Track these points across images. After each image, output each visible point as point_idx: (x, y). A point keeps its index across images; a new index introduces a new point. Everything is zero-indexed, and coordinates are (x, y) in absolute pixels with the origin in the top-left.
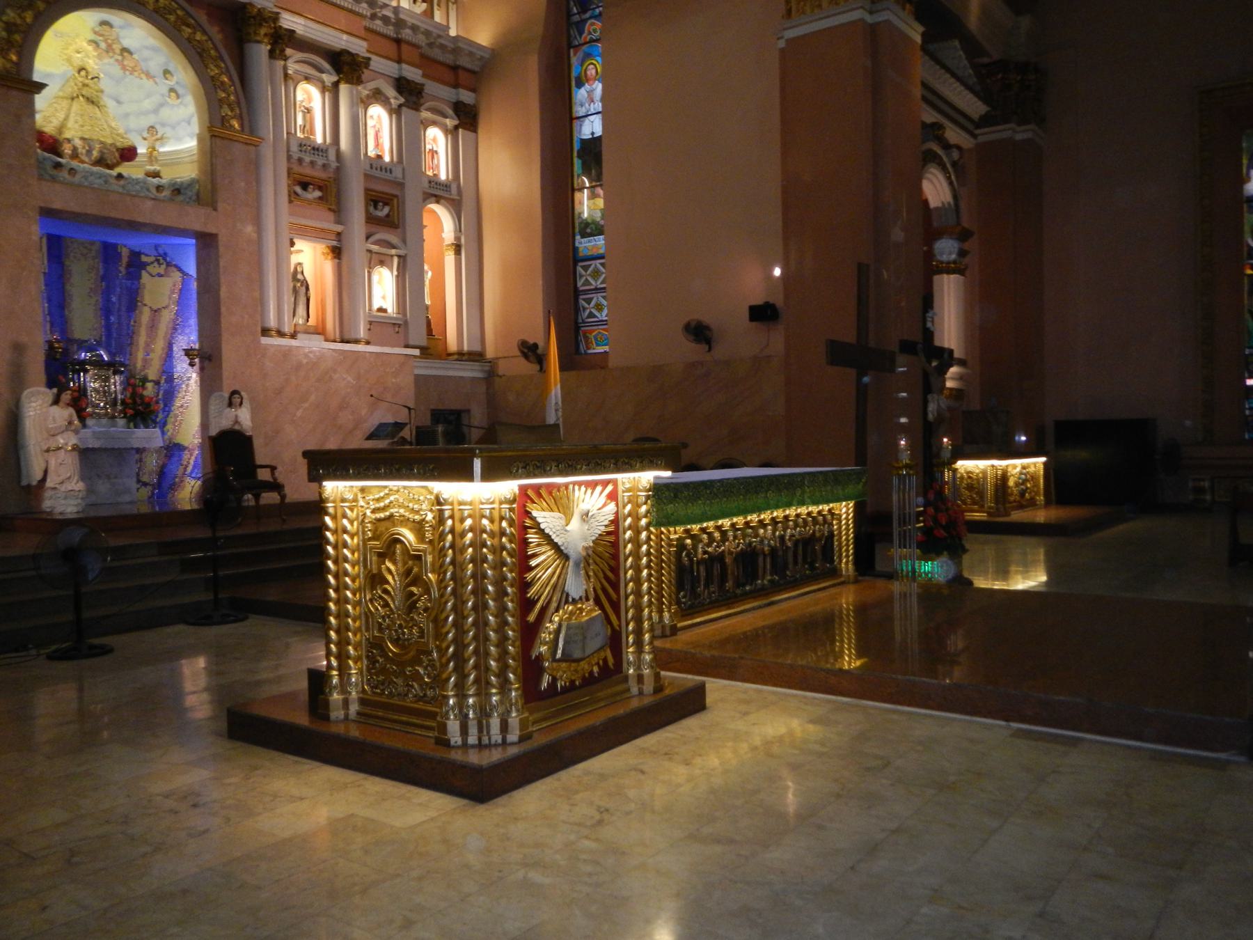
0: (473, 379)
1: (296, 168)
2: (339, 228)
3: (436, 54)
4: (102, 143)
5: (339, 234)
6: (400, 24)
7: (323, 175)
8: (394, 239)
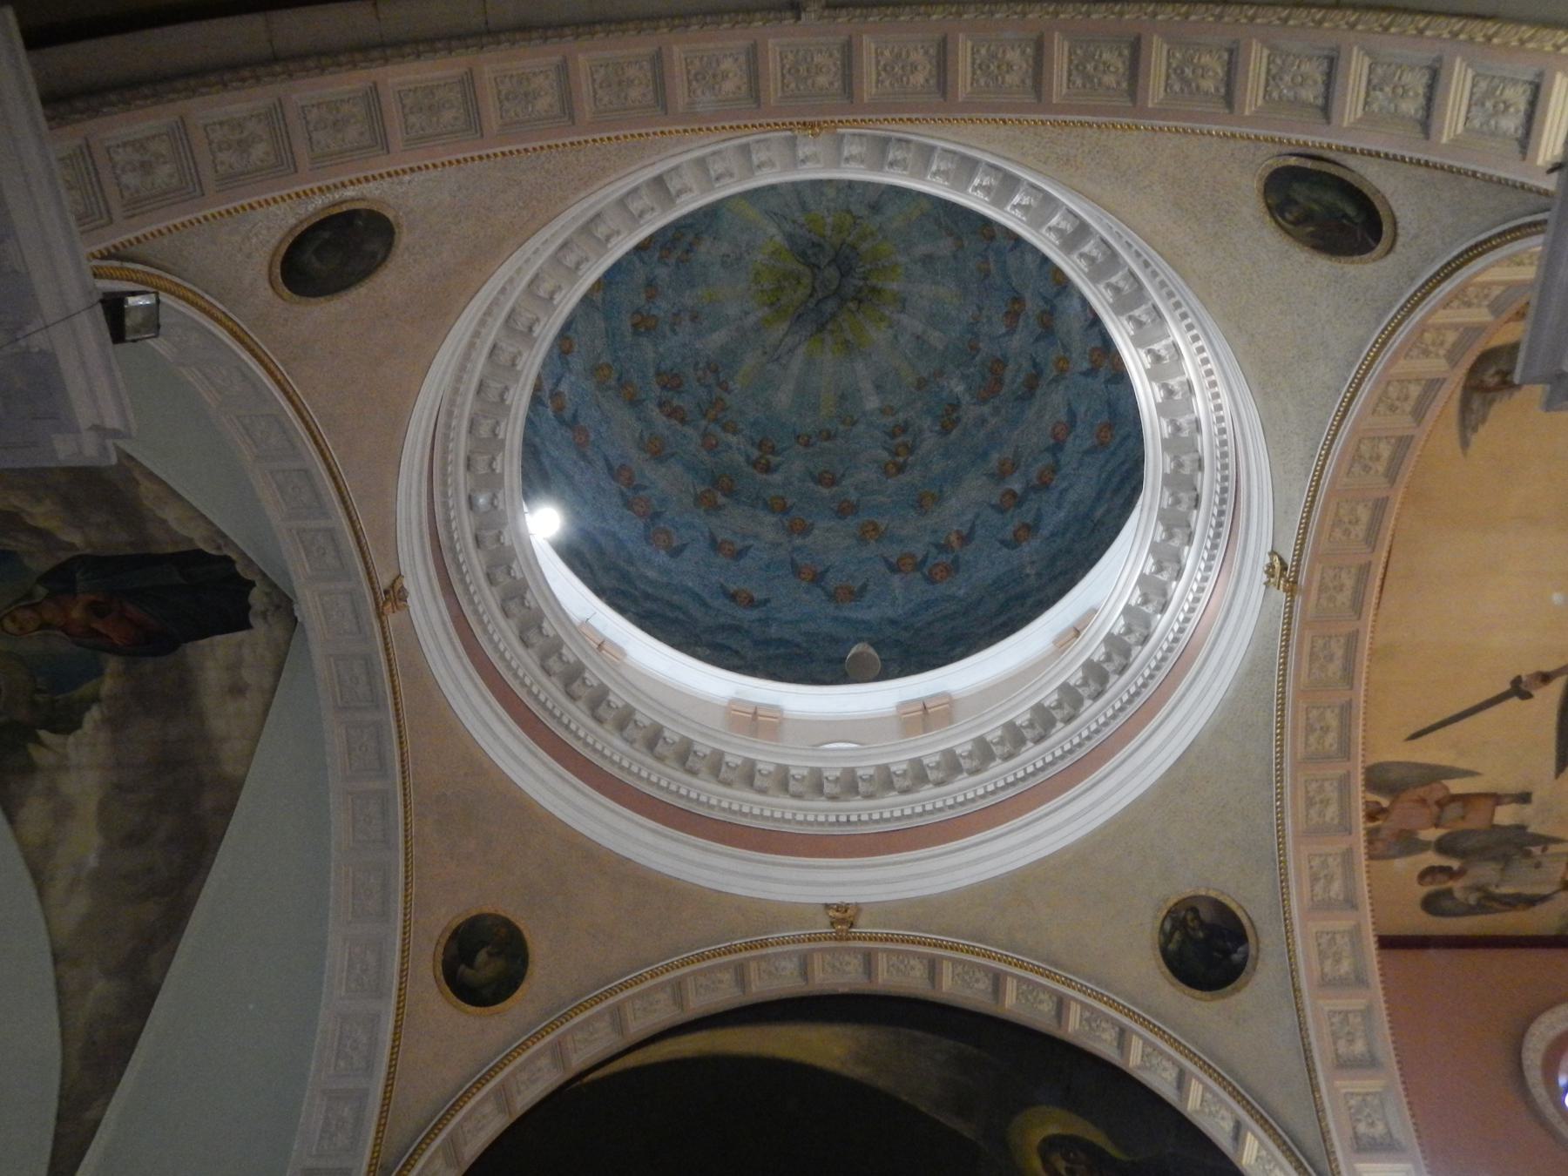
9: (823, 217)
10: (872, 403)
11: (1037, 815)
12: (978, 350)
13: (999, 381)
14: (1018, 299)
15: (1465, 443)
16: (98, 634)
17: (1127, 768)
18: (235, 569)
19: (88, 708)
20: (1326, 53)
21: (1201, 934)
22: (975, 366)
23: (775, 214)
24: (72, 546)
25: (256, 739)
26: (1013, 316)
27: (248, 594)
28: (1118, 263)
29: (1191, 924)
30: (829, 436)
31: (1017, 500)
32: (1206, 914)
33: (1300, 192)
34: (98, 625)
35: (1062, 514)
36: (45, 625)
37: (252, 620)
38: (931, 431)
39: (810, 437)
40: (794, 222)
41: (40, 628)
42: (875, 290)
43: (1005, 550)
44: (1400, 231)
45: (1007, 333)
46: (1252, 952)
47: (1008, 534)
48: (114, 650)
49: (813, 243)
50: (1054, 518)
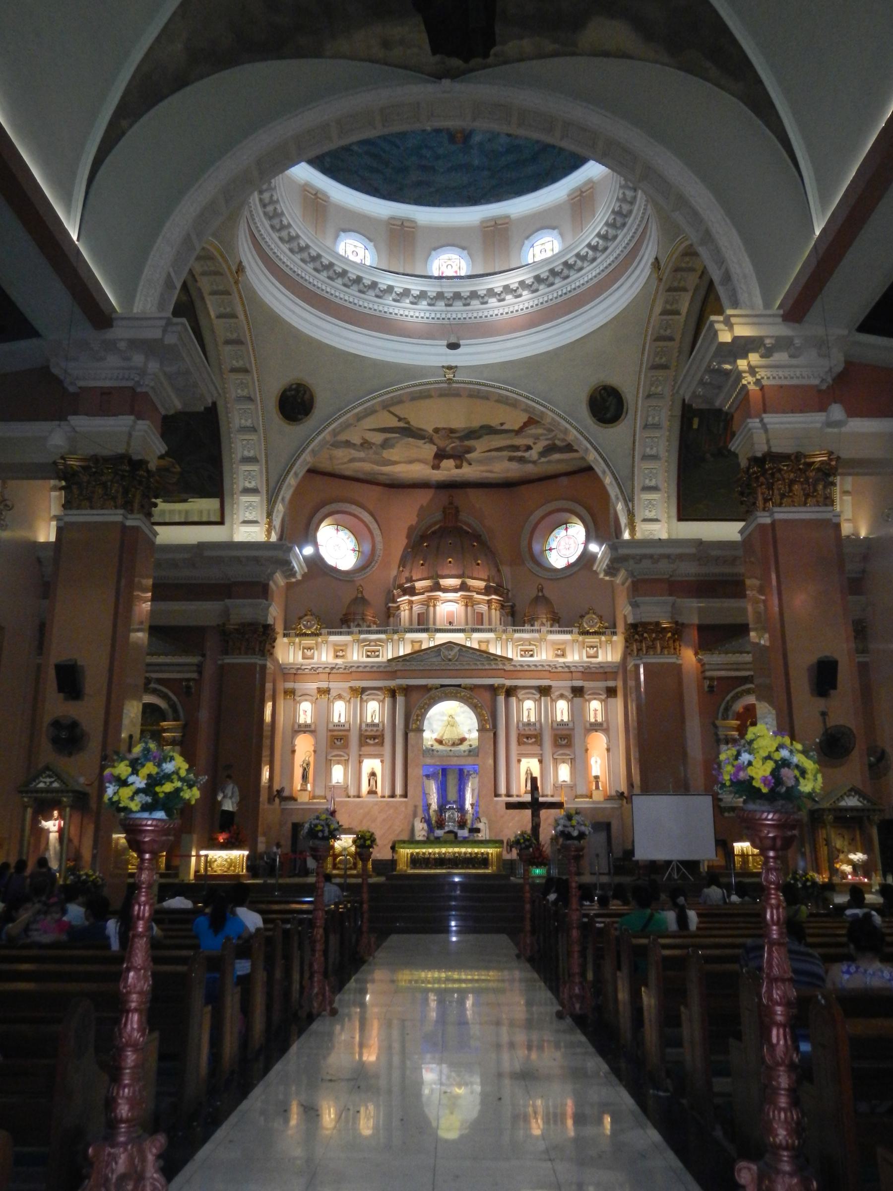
0: (613, 808)
1: (523, 733)
2: (541, 752)
3: (594, 670)
4: (452, 739)
5: (541, 754)
6: (568, 667)
7: (534, 733)
8: (568, 752)
21: (299, 400)
25: (353, 58)
32: (307, 396)
37: (438, 57)
46: (304, 420)
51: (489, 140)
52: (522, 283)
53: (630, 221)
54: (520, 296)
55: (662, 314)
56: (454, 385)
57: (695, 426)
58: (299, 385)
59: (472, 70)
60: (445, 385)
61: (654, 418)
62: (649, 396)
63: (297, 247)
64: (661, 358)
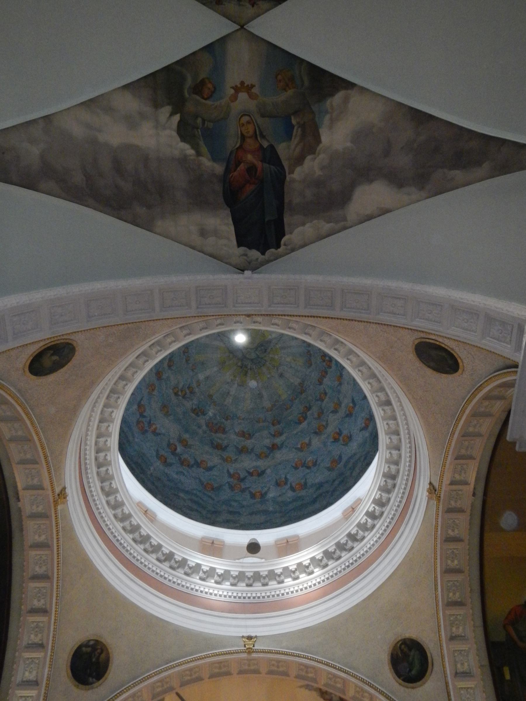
9: (278, 355)
10: (201, 377)
11: (113, 559)
12: (227, 420)
13: (216, 432)
14: (250, 436)
15: (301, 687)
16: (237, 165)
17: (145, 593)
18: (273, 248)
19: (193, 148)
20: (471, 670)
22: (220, 420)
23: (281, 338)
24: (292, 172)
26: (243, 434)
27: (258, 250)
28: (342, 551)
29: (96, 653)
30: (187, 361)
31: (174, 452)
32: (103, 656)
33: (414, 654)
34: (242, 167)
35: (175, 476)
36: (243, 137)
37: (242, 249)
38: (192, 404)
39: (187, 353)
40: (277, 344)
41: (242, 135)
42: (246, 374)
43: (155, 454)
44: (410, 689)
45: (235, 433)
47: (162, 452)
48: (227, 170)
49: (266, 349)
50: (172, 472)
51: (280, 496)
52: (313, 559)
53: (399, 480)
54: (312, 573)
55: (452, 483)
56: (254, 655)
57: (508, 677)
58: (97, 642)
59: (268, 261)
60: (244, 655)
61: (462, 664)
62: (452, 638)
63: (121, 513)
64: (454, 594)
